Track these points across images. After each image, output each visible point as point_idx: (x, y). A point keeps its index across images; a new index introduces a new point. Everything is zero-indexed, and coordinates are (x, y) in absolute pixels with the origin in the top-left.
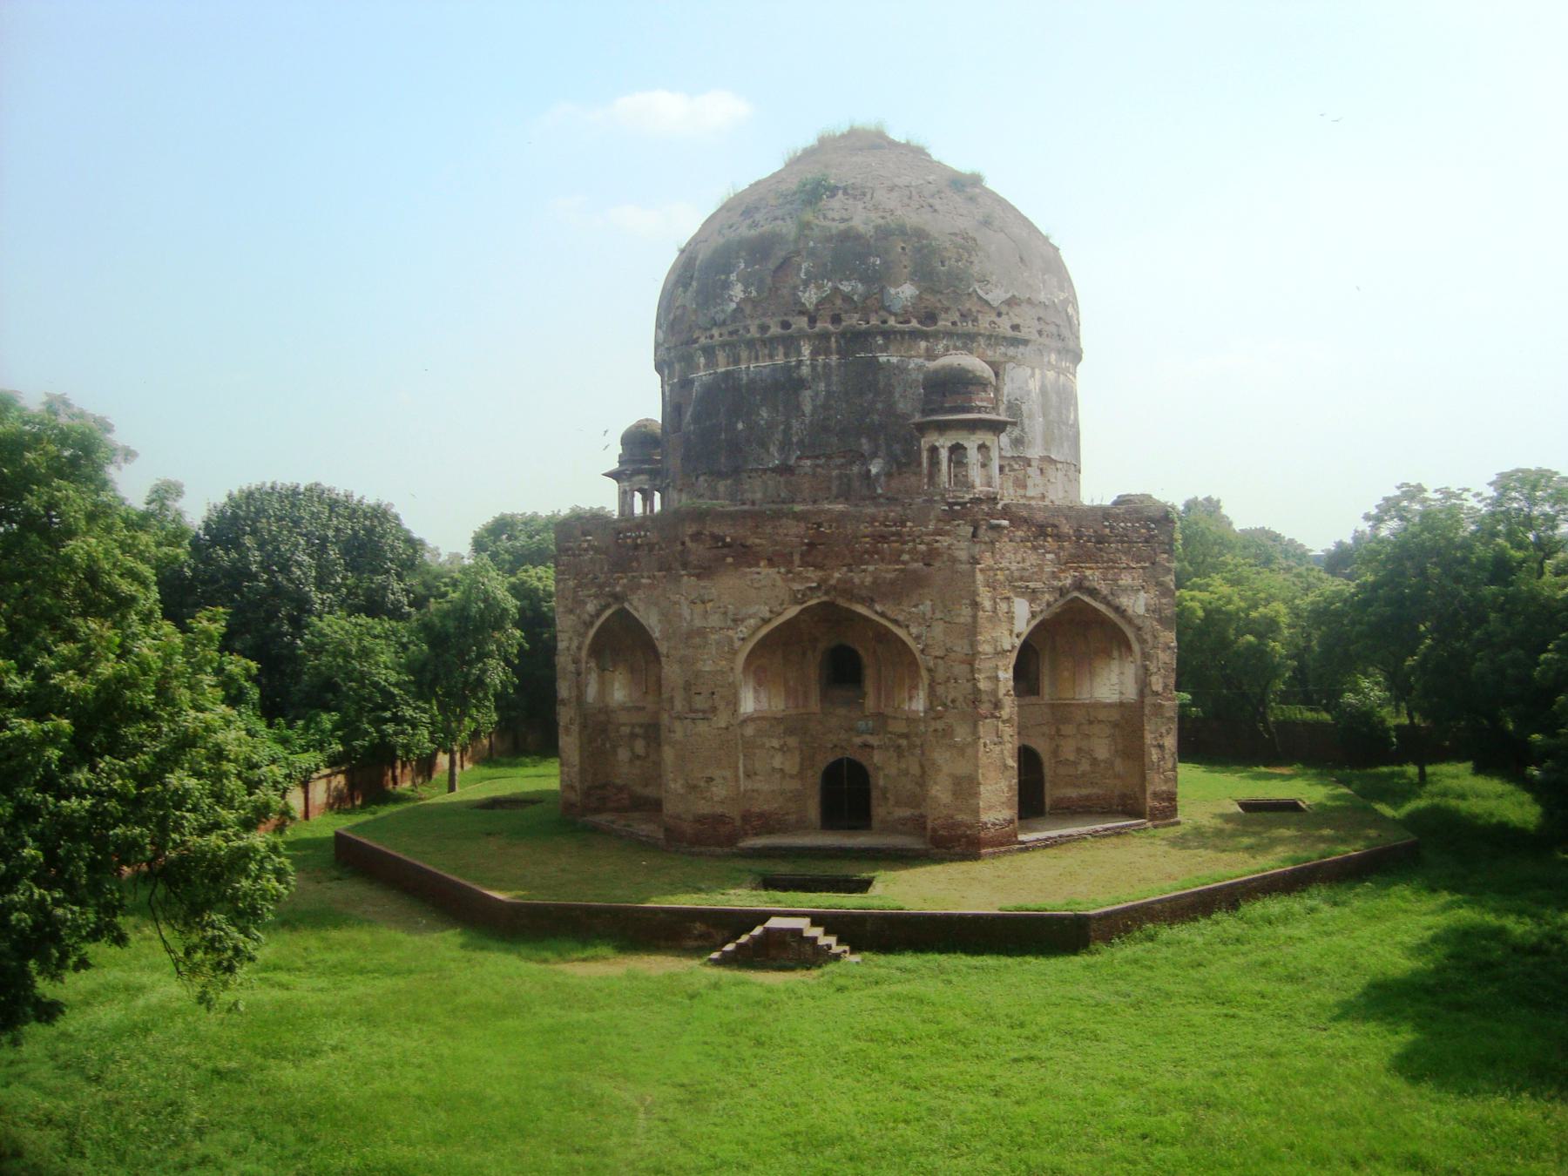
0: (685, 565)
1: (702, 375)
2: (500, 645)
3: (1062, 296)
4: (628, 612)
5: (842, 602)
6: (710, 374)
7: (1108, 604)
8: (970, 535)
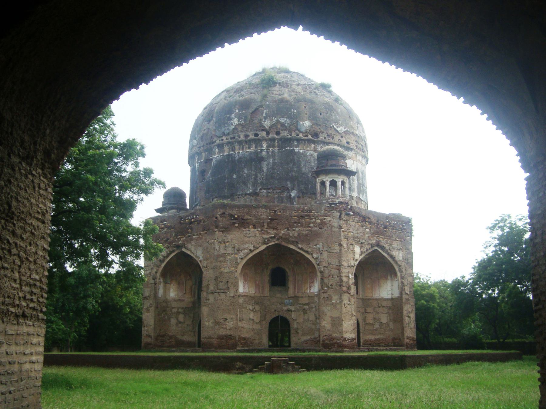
0: (217, 227)
1: (216, 156)
2: (93, 292)
3: (364, 135)
4: (184, 252)
5: (284, 244)
6: (220, 156)
7: (388, 254)
8: (338, 217)
